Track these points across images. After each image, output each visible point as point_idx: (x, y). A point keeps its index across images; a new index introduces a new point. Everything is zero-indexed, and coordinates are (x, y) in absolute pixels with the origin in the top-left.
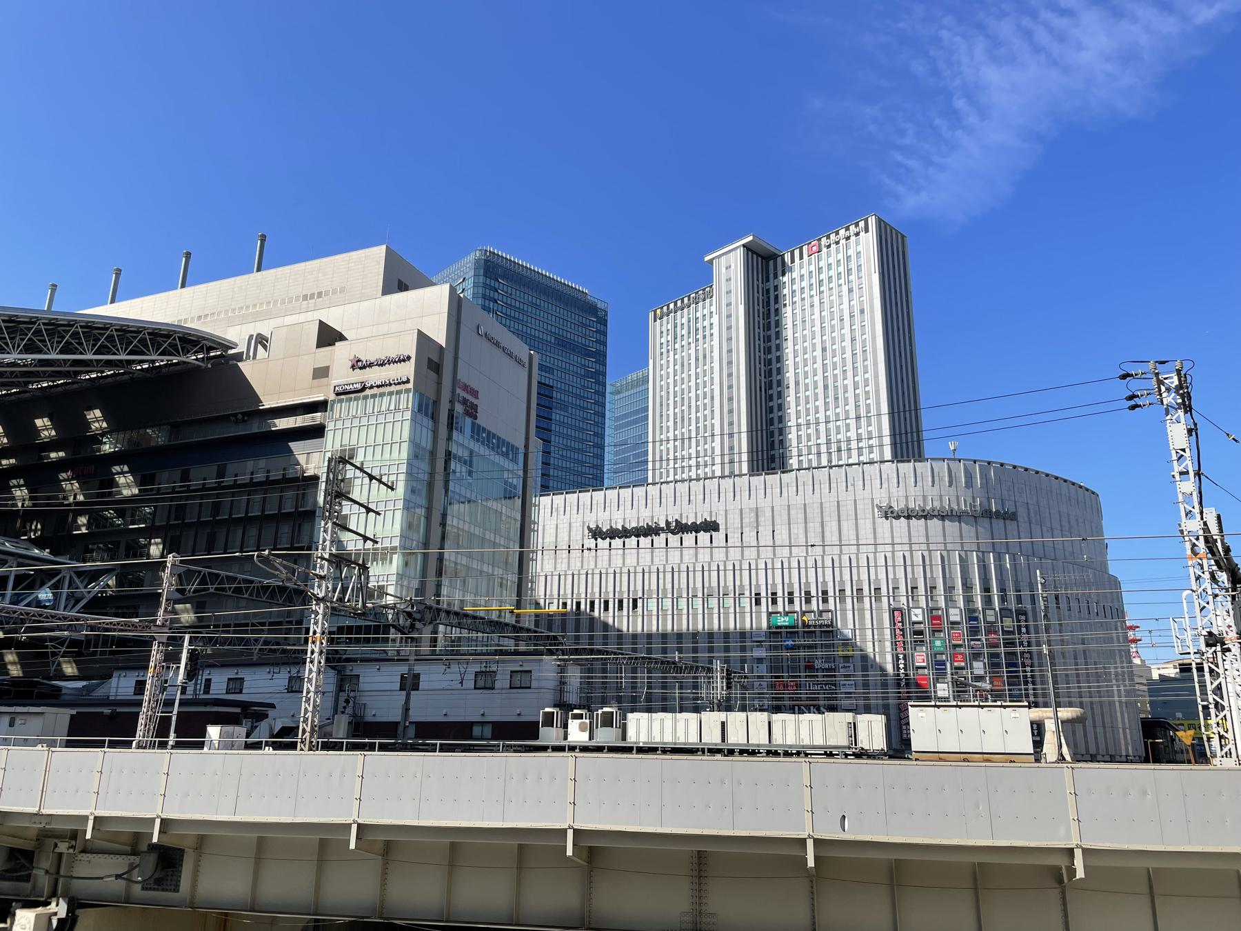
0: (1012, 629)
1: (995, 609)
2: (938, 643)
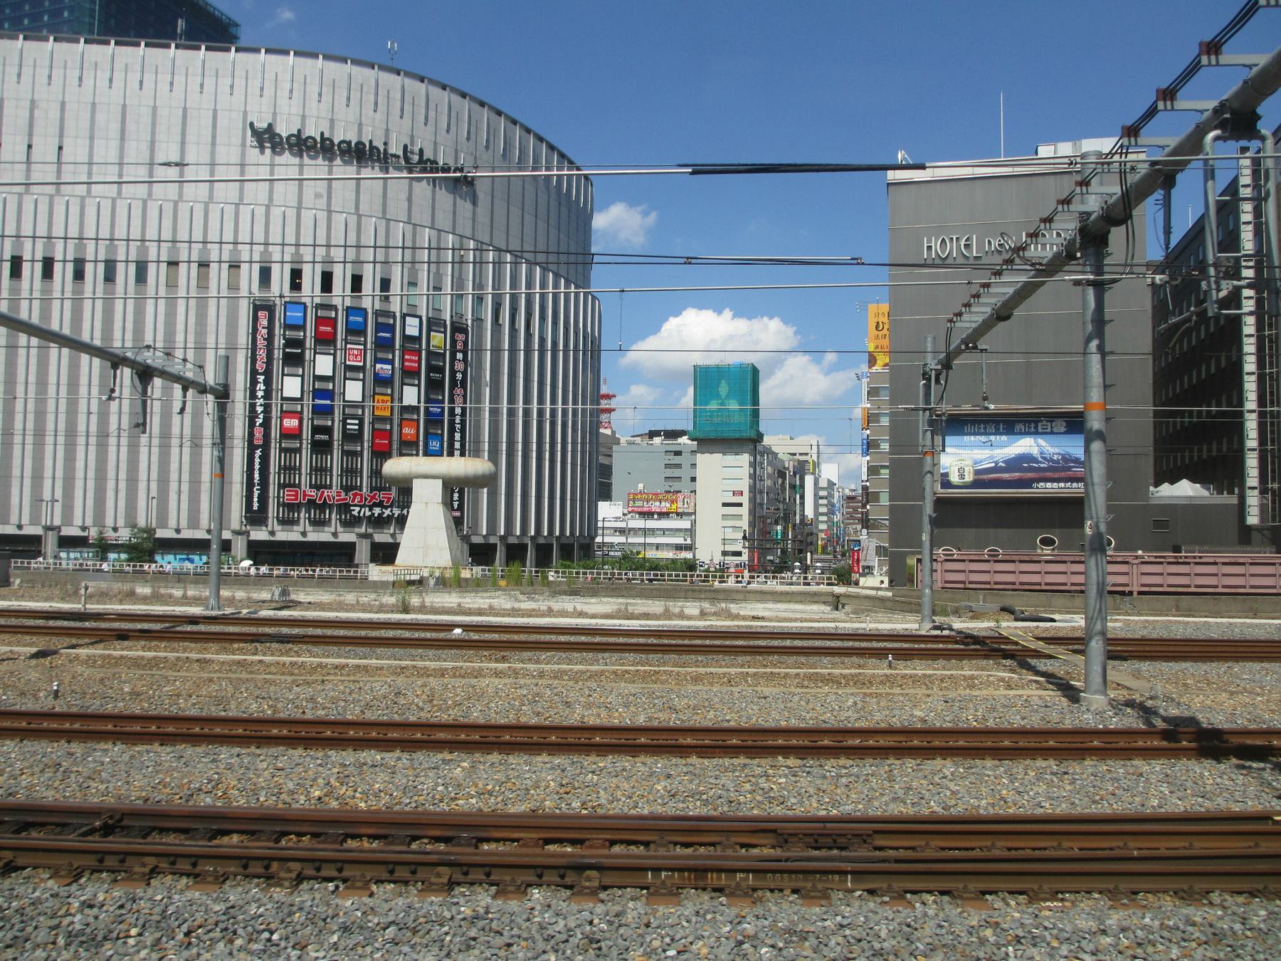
1: (420, 317)
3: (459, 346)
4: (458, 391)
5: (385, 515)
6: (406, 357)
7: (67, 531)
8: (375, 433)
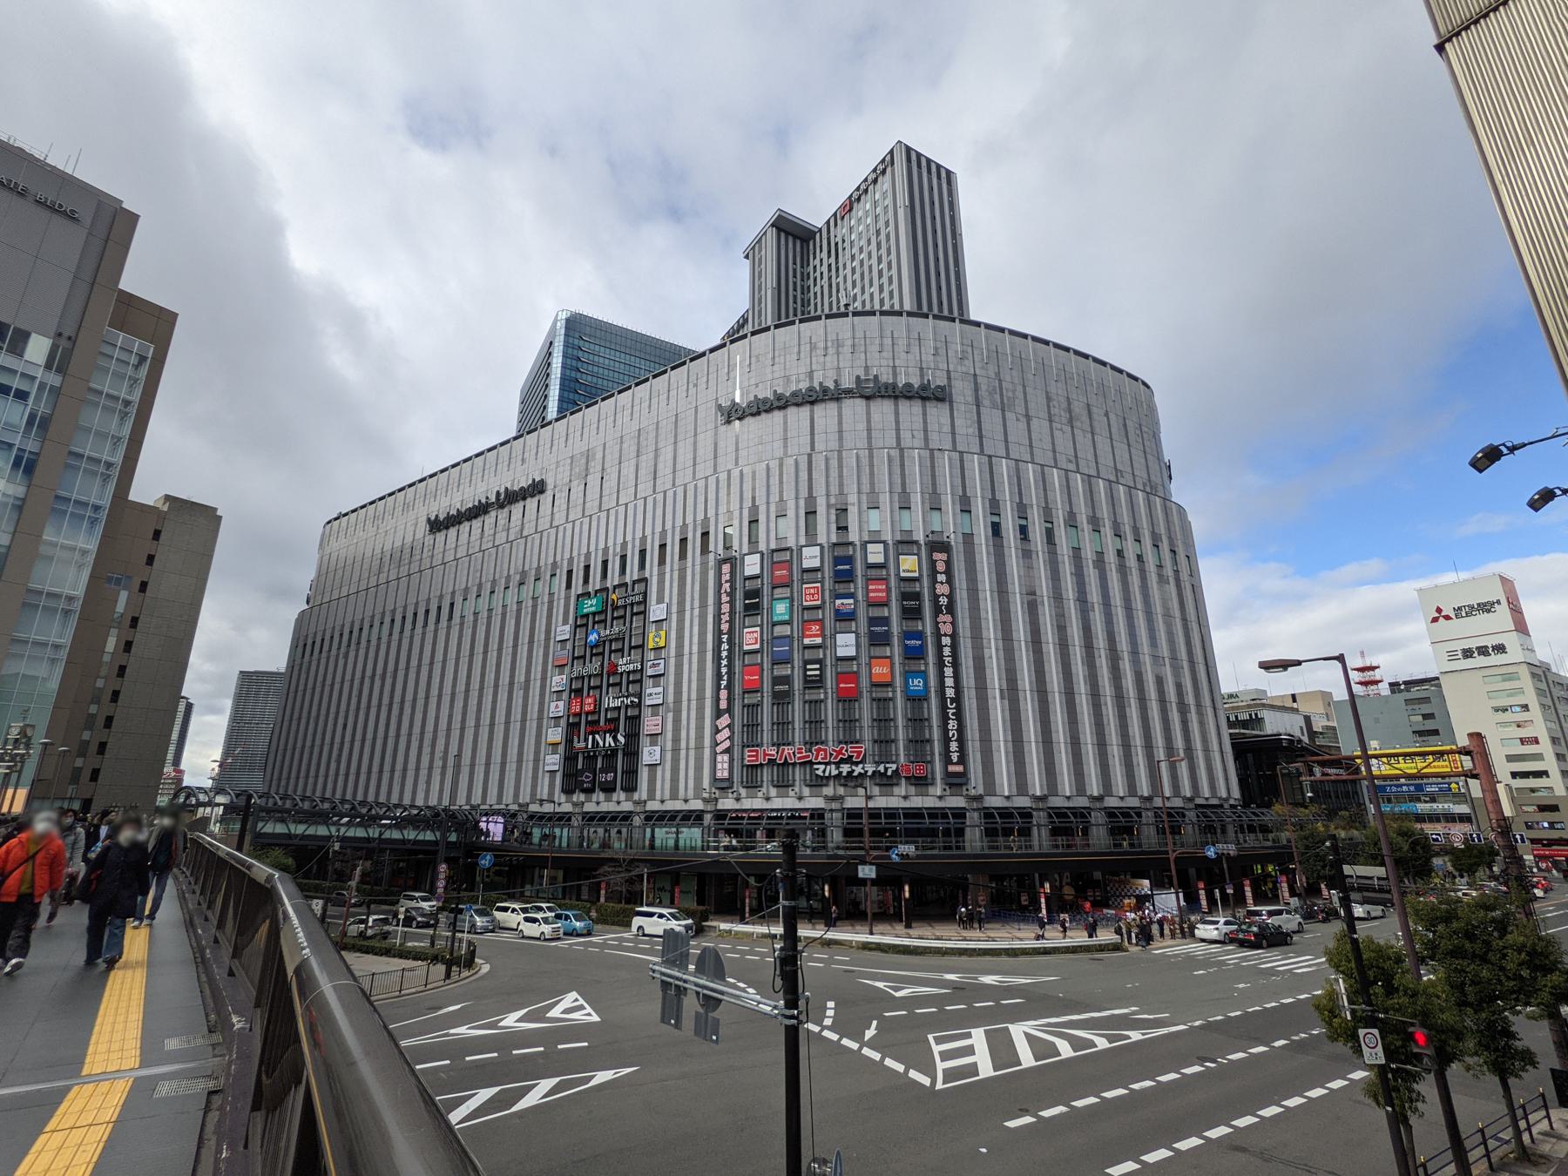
0: (916, 575)
2: (781, 609)
3: (941, 567)
5: (855, 774)
6: (870, 587)
7: (653, 806)
8: (841, 677)
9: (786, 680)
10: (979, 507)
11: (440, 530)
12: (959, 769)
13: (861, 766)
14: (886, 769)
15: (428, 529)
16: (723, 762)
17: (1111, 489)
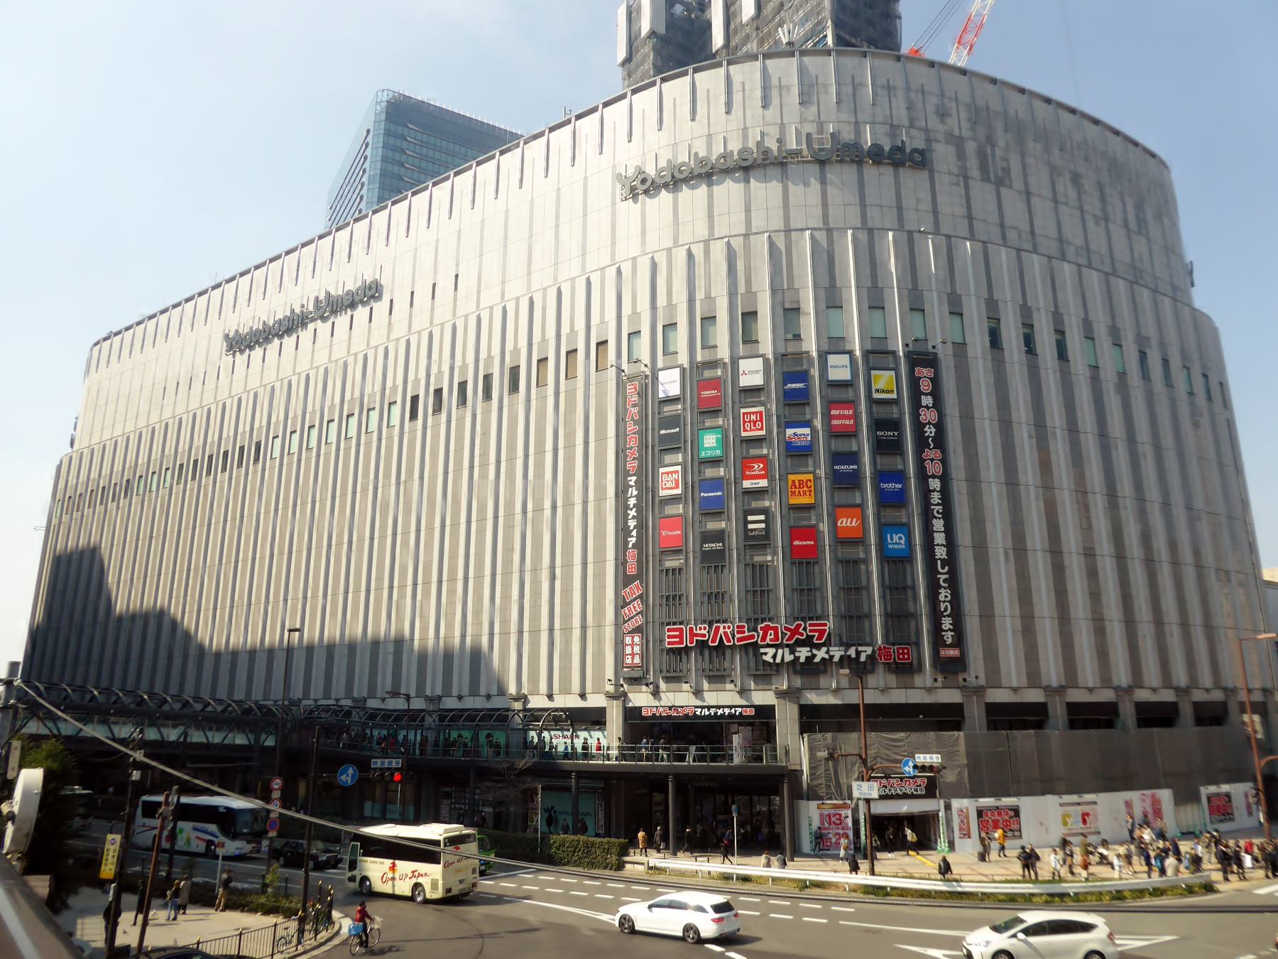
0: (894, 396)
1: (850, 353)
2: (710, 442)
3: (926, 386)
4: (931, 453)
5: (817, 660)
6: (833, 412)
9: (720, 536)
10: (974, 309)
11: (242, 352)
12: (954, 653)
13: (824, 649)
14: (858, 653)
15: (225, 348)
16: (632, 645)
17: (1133, 293)
